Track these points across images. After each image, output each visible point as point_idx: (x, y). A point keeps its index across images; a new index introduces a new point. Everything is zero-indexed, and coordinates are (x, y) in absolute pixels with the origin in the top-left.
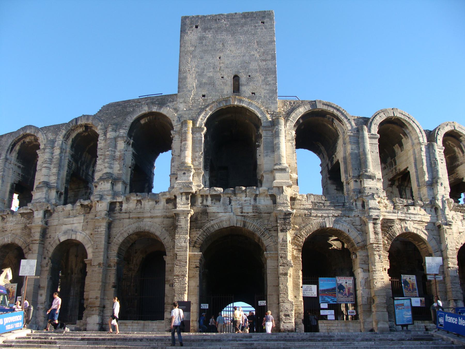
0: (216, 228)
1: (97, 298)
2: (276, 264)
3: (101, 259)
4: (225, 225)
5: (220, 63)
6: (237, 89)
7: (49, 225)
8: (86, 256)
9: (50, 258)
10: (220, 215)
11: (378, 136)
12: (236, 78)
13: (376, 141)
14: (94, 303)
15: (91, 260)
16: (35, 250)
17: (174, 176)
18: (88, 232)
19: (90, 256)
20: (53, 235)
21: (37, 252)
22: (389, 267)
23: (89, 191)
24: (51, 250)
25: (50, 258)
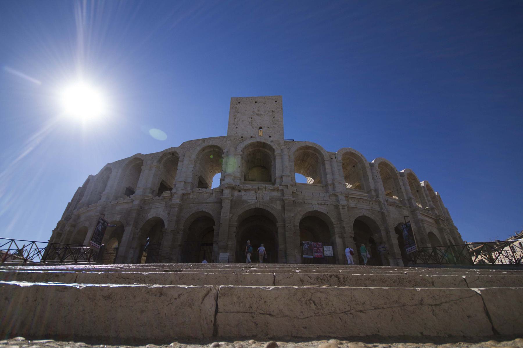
4: (253, 207)
10: (249, 201)
17: (222, 180)
18: (166, 212)
19: (166, 227)
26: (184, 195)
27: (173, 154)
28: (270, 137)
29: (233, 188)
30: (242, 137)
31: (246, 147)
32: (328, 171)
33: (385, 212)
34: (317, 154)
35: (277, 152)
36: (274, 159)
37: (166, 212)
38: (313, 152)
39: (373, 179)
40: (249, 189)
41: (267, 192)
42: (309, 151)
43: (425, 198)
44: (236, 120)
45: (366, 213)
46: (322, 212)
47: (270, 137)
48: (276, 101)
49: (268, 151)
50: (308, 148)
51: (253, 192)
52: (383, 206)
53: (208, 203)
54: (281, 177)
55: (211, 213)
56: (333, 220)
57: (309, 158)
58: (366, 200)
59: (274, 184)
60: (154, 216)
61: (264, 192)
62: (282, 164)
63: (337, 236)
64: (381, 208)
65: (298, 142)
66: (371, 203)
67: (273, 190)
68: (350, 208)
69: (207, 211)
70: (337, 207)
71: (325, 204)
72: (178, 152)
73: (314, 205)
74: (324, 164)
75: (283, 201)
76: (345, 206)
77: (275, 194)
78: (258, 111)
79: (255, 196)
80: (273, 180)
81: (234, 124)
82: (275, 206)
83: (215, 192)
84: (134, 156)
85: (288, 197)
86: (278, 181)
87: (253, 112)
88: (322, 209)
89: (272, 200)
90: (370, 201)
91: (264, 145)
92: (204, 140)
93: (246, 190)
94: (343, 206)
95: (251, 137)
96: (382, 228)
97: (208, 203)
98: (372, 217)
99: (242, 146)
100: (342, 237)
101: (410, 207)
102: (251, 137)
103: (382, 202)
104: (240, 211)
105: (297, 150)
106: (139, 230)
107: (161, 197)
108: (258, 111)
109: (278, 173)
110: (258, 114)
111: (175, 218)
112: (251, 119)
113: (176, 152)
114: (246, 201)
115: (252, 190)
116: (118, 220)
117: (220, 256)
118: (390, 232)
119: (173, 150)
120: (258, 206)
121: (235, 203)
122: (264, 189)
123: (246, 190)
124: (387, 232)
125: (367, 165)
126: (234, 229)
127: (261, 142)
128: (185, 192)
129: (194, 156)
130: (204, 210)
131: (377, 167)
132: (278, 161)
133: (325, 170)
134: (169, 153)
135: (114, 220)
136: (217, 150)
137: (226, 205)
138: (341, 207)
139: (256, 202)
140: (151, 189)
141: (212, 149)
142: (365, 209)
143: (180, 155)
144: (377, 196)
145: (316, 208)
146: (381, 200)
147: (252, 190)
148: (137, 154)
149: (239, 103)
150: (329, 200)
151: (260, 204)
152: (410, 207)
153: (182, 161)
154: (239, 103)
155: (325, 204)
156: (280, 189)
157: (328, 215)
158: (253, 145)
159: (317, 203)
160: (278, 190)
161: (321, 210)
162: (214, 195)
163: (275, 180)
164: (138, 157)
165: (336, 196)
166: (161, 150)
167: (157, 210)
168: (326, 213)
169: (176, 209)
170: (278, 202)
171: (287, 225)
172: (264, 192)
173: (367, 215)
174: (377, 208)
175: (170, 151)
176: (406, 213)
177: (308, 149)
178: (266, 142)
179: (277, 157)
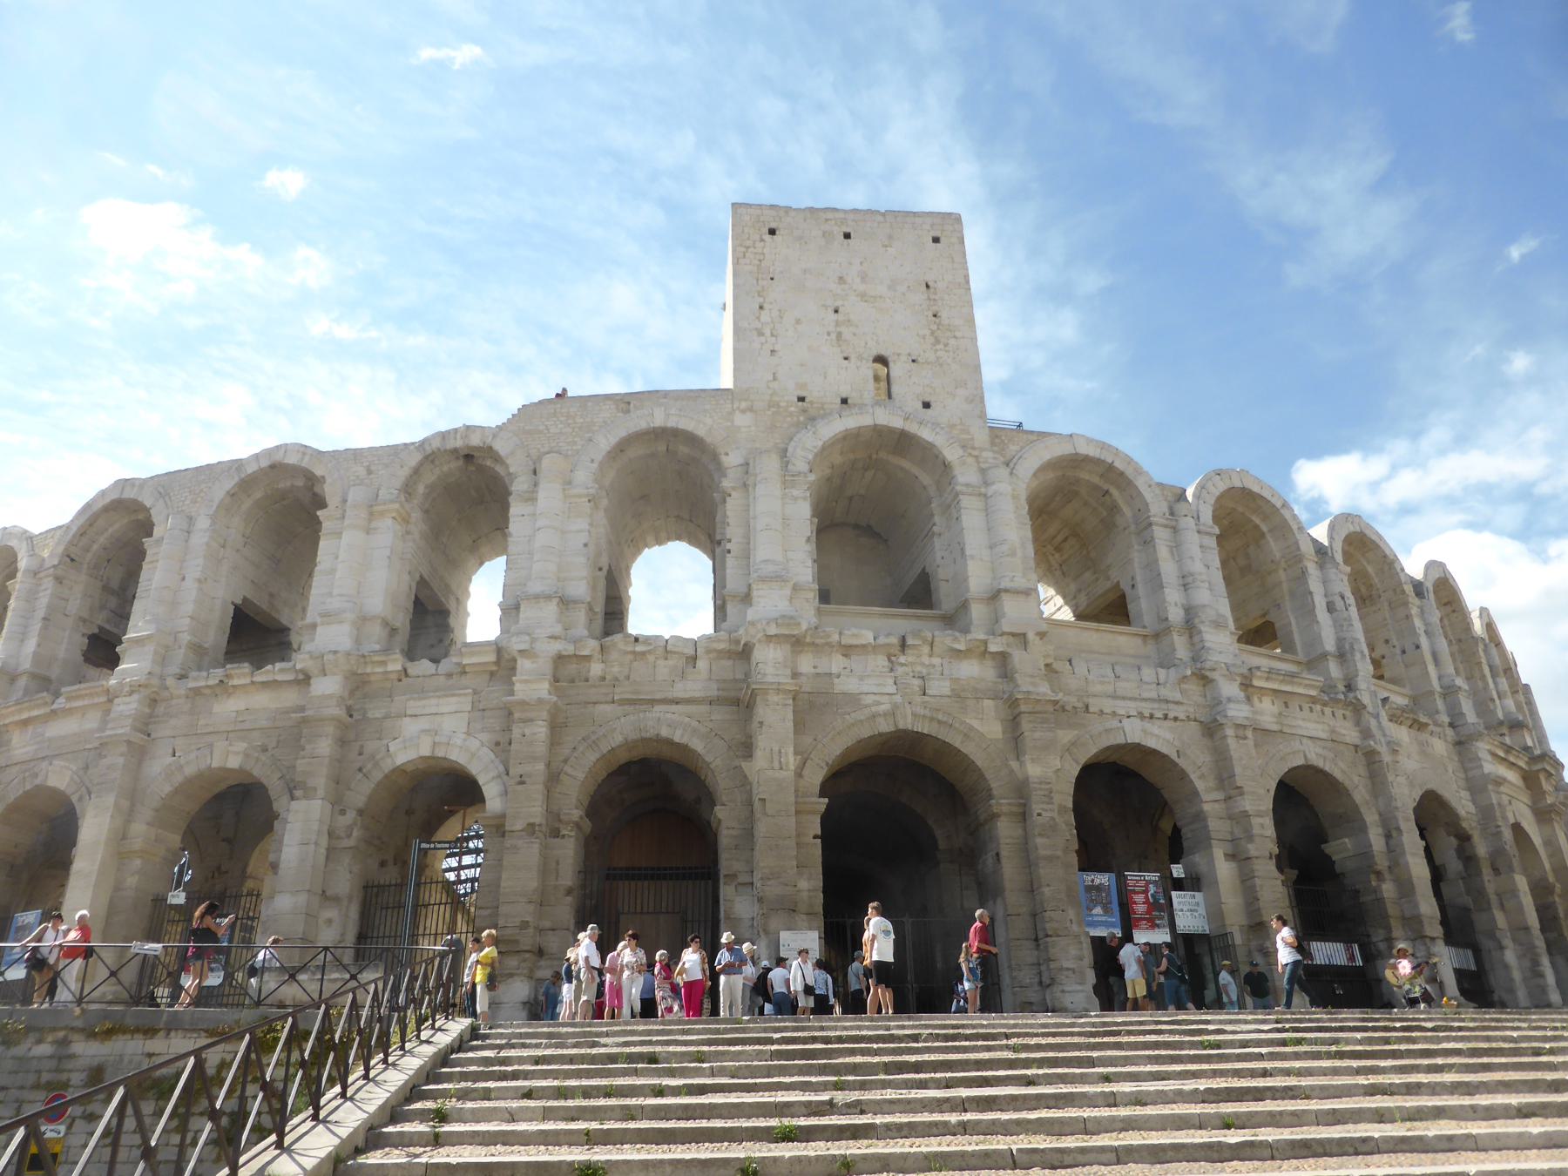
1: (524, 925)
2: (1020, 832)
4: (885, 727)
5: (837, 324)
7: (356, 716)
9: (360, 812)
10: (869, 700)
11: (1217, 531)
13: (1213, 543)
14: (516, 942)
15: (503, 816)
16: (315, 789)
18: (485, 737)
20: (371, 746)
21: (321, 792)
22: (1276, 851)
25: (360, 812)
26: (560, 659)
27: (468, 457)
28: (927, 405)
29: (797, 643)
30: (801, 399)
31: (826, 449)
32: (1168, 569)
33: (1383, 750)
34: (1115, 492)
35: (965, 475)
36: (951, 508)
37: (485, 737)
38: (1096, 480)
39: (1330, 608)
40: (864, 646)
41: (936, 661)
42: (1084, 476)
43: (1490, 681)
44: (765, 316)
45: (1315, 755)
46: (1154, 752)
47: (927, 405)
48: (936, 240)
49: (915, 470)
50: (1077, 461)
51: (882, 661)
52: (1373, 722)
53: (676, 702)
54: (995, 596)
55: (697, 745)
56: (1200, 785)
57: (1083, 514)
58: (1314, 700)
59: (966, 631)
60: (425, 751)
61: (926, 660)
62: (988, 540)
63: (1218, 853)
64: (1366, 734)
66: (1328, 710)
67: (957, 654)
68: (1262, 732)
69: (677, 739)
70: (1211, 729)
71: (1166, 717)
72: (501, 447)
73: (1125, 721)
74: (1148, 543)
75: (1013, 703)
76: (1244, 727)
77: (970, 670)
78: (864, 278)
79: (885, 680)
81: (761, 334)
82: (976, 724)
83: (708, 651)
84: (269, 452)
85: (1031, 684)
86: (977, 612)
87: (841, 279)
88: (1159, 738)
89: (959, 695)
91: (903, 442)
92: (625, 402)
94: (1238, 726)
95: (844, 401)
96: (1371, 818)
97: (676, 702)
99: (808, 444)
100: (1236, 856)
101: (1451, 725)
102: (844, 401)
103: (1370, 708)
104: (833, 745)
106: (351, 816)
107: (445, 665)
109: (977, 579)
110: (863, 296)
111: (541, 767)
112: (834, 317)
113: (489, 451)
114: (853, 700)
115: (874, 649)
116: (234, 763)
118: (1398, 829)
119: (475, 441)
120: (907, 722)
121: (811, 706)
122: (926, 649)
123: (847, 650)
124: (1391, 833)
125: (1307, 549)
127: (891, 430)
128: (569, 649)
129: (584, 477)
130: (665, 732)
131: (1339, 557)
132: (971, 518)
133: (1152, 566)
134: (455, 451)
135: (215, 764)
136: (683, 450)
137: (775, 720)
138: (1230, 732)
139: (895, 706)
140: (385, 623)
141: (662, 448)
142: (1314, 738)
143: (516, 465)
144: (1350, 687)
145: (1134, 732)
146: (1366, 699)
147: (874, 649)
148: (283, 448)
150: (1178, 696)
151: (914, 715)
152: (1451, 725)
153: (531, 498)
154: (772, 232)
155: (1166, 717)
156: (993, 648)
157: (1181, 762)
158: (851, 439)
159: (1132, 705)
160: (985, 653)
161: (1151, 743)
162: (702, 664)
163: (964, 606)
164: (292, 460)
165: (1204, 680)
166: (416, 436)
167: (433, 726)
168: (1174, 756)
169: (540, 730)
170: (988, 703)
171: (1036, 808)
172: (926, 660)
173: (1320, 764)
174: (1350, 734)
175: (459, 443)
176: (1440, 747)
178: (912, 428)
179: (965, 501)
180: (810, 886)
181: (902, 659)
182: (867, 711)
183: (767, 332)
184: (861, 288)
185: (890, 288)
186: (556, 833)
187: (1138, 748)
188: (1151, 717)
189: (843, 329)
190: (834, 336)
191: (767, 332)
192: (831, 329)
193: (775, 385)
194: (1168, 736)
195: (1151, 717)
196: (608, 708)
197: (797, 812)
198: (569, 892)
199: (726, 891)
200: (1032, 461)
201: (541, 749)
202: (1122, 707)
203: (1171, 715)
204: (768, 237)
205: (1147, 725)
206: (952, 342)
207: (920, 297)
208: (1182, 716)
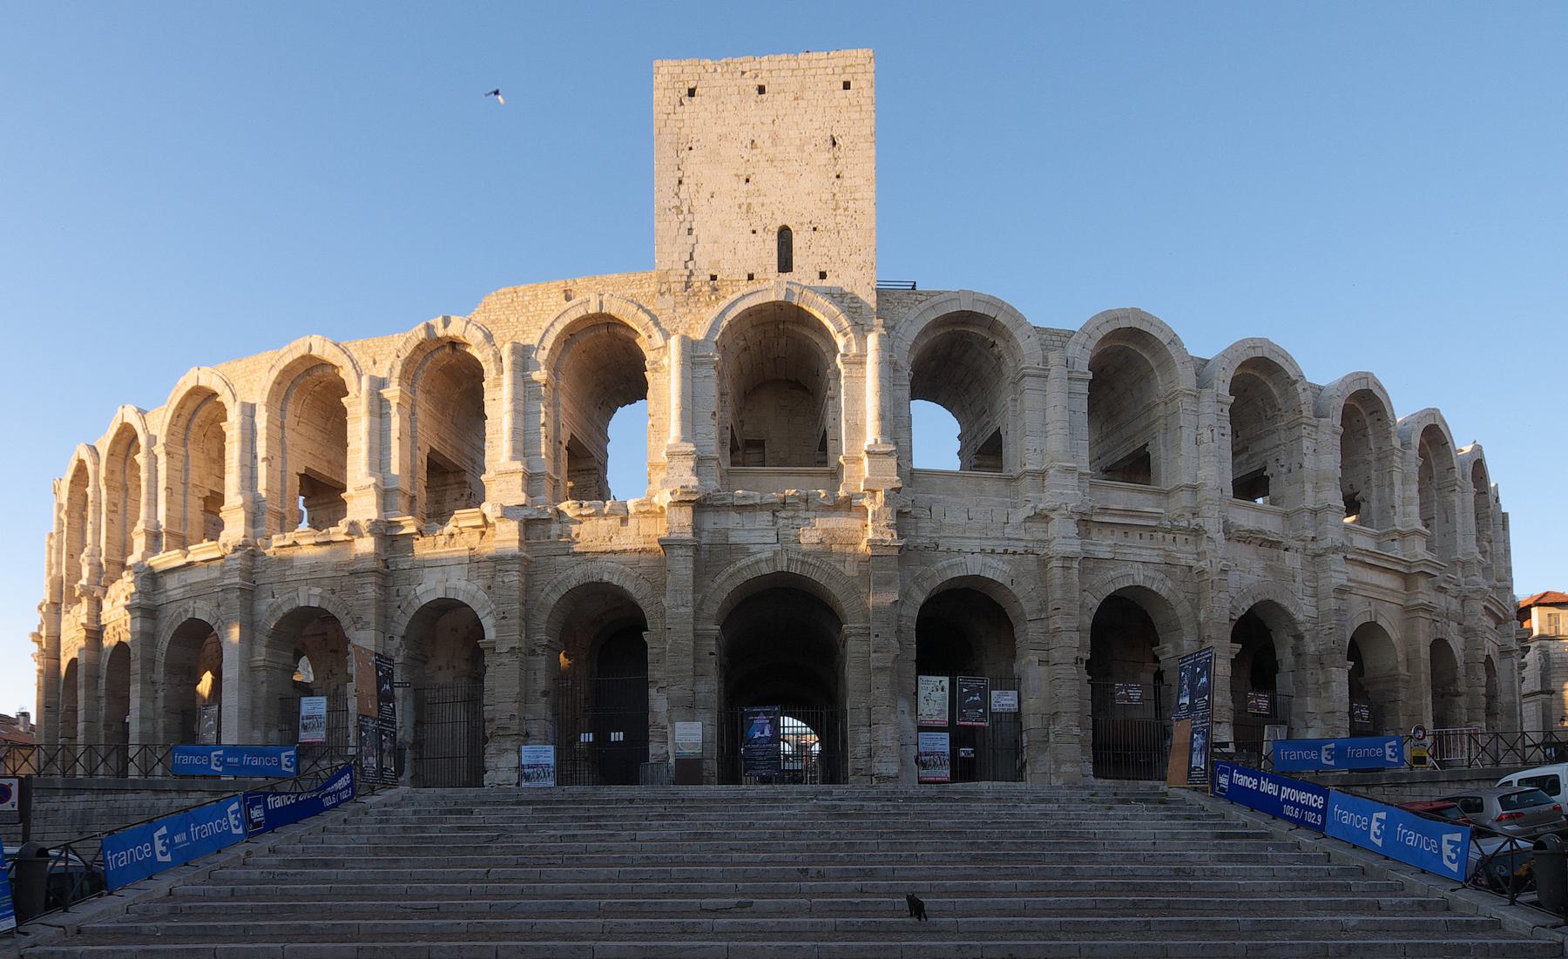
0: (748, 575)
3: (515, 638)
4: (766, 570)
6: (785, 264)
8: (479, 630)
10: (754, 549)
12: (785, 235)
13: (1084, 388)
23: (468, 491)
24: (405, 621)
30: (714, 278)
55: (629, 587)
65: (930, 294)
68: (1089, 562)
78: (775, 139)
80: (832, 465)
90: (1169, 531)
93: (741, 508)
98: (1162, 587)
102: (751, 277)
104: (724, 586)
105: (924, 332)
108: (775, 139)
114: (742, 549)
117: (677, 732)
120: (782, 566)
122: (802, 506)
123: (741, 508)
126: (711, 645)
130: (606, 578)
142: (1136, 564)
145: (974, 566)
149: (692, 93)
155: (1006, 552)
157: (1015, 590)
161: (989, 574)
177: (964, 323)
180: (710, 687)
181: (783, 514)
182: (752, 559)
183: (685, 209)
184: (771, 151)
185: (801, 149)
186: (533, 652)
187: (977, 578)
188: (993, 552)
189: (755, 201)
190: (744, 208)
191: (685, 209)
192: (742, 200)
193: (690, 265)
194: (1006, 568)
195: (993, 552)
196: (564, 559)
197: (696, 635)
198: (545, 694)
199: (652, 692)
200: (913, 325)
201: (516, 594)
202: (968, 545)
203: (1011, 550)
204: (686, 100)
205: (988, 560)
206: (851, 205)
207: (825, 157)
208: (1020, 550)
